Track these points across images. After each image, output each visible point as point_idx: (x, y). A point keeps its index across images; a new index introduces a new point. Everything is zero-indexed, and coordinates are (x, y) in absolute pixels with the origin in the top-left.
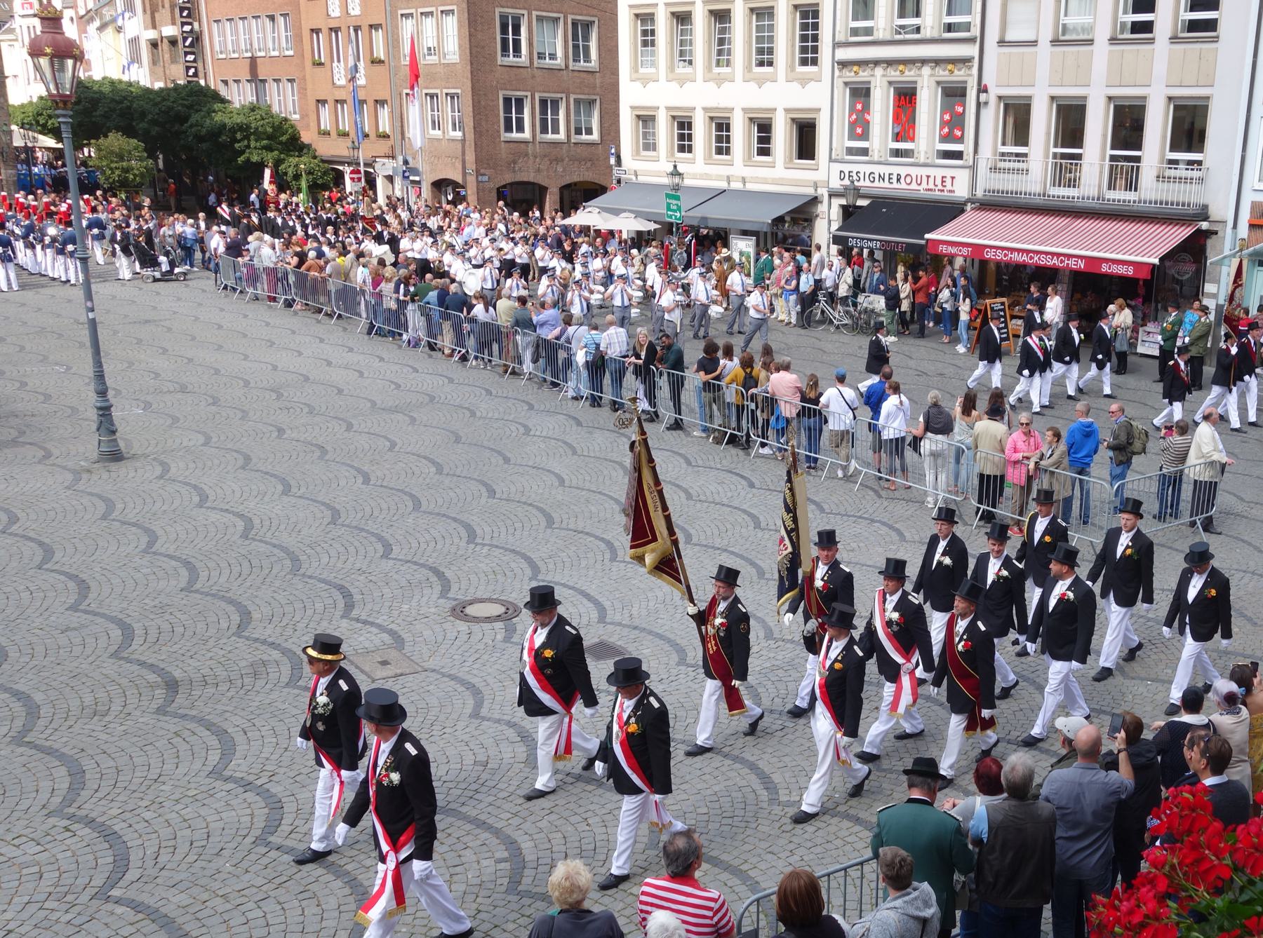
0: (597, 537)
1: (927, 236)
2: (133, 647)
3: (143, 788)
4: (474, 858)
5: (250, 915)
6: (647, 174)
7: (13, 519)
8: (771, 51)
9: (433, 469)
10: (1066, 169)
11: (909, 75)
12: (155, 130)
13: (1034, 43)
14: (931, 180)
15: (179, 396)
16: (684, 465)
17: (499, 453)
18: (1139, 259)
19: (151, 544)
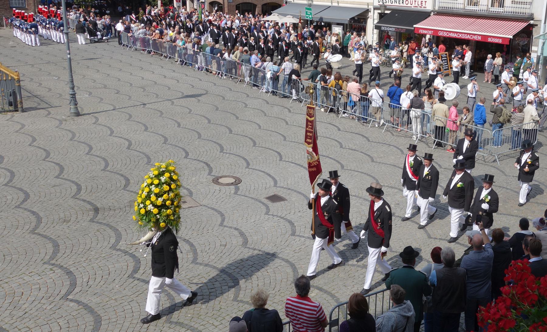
0: (274, 151)
1: (414, 26)
7: (34, 140)
9: (207, 121)
14: (416, 3)
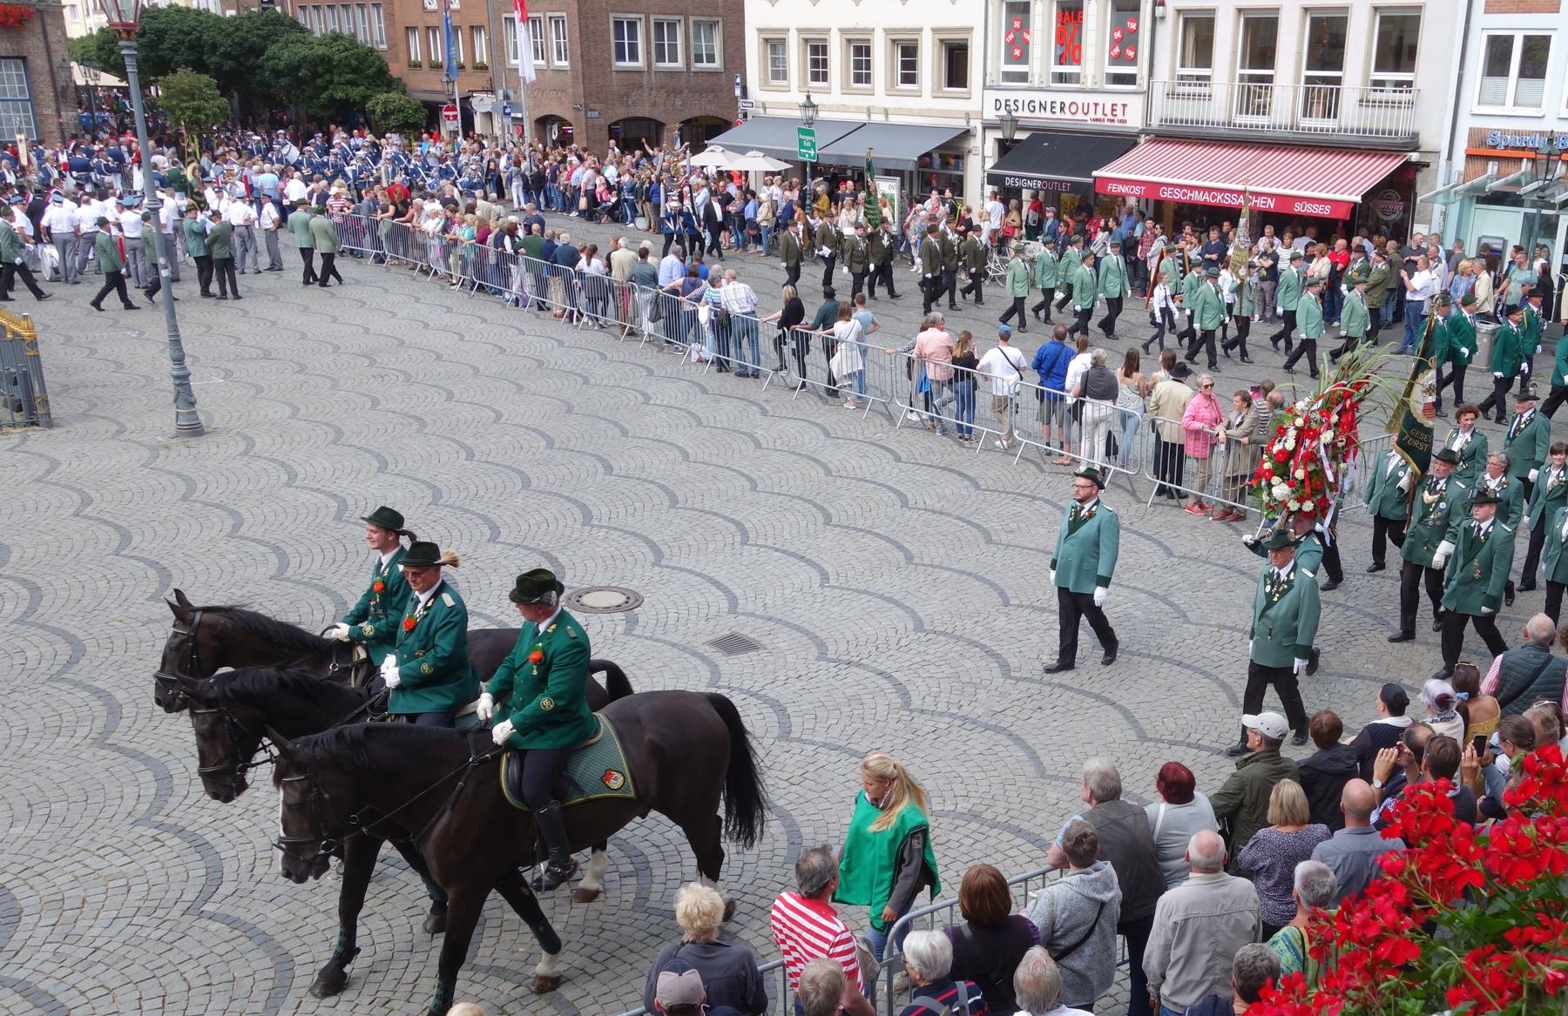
1: (1095, 173)
6: (777, 106)
7: (87, 501)
9: (543, 443)
10: (1256, 91)
12: (228, 65)
14: (1100, 109)
15: (263, 363)
16: (822, 437)
17: (615, 424)
18: (1338, 197)
19: (237, 527)
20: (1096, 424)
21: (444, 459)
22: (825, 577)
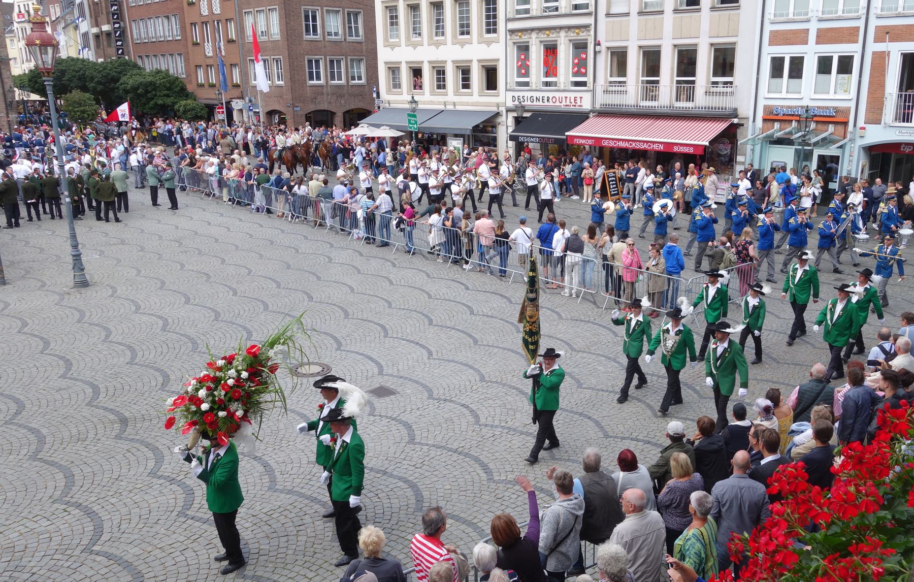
0: (375, 323)
2: (100, 399)
3: (109, 484)
4: (310, 520)
5: (178, 559)
7: (25, 324)
8: (468, 26)
10: (650, 89)
11: (553, 36)
12: (100, 88)
13: (627, 14)
14: (568, 100)
15: (121, 246)
16: (426, 278)
17: (314, 274)
18: (696, 143)
19: (107, 336)
20: (573, 266)
21: (221, 295)
22: (430, 353)
